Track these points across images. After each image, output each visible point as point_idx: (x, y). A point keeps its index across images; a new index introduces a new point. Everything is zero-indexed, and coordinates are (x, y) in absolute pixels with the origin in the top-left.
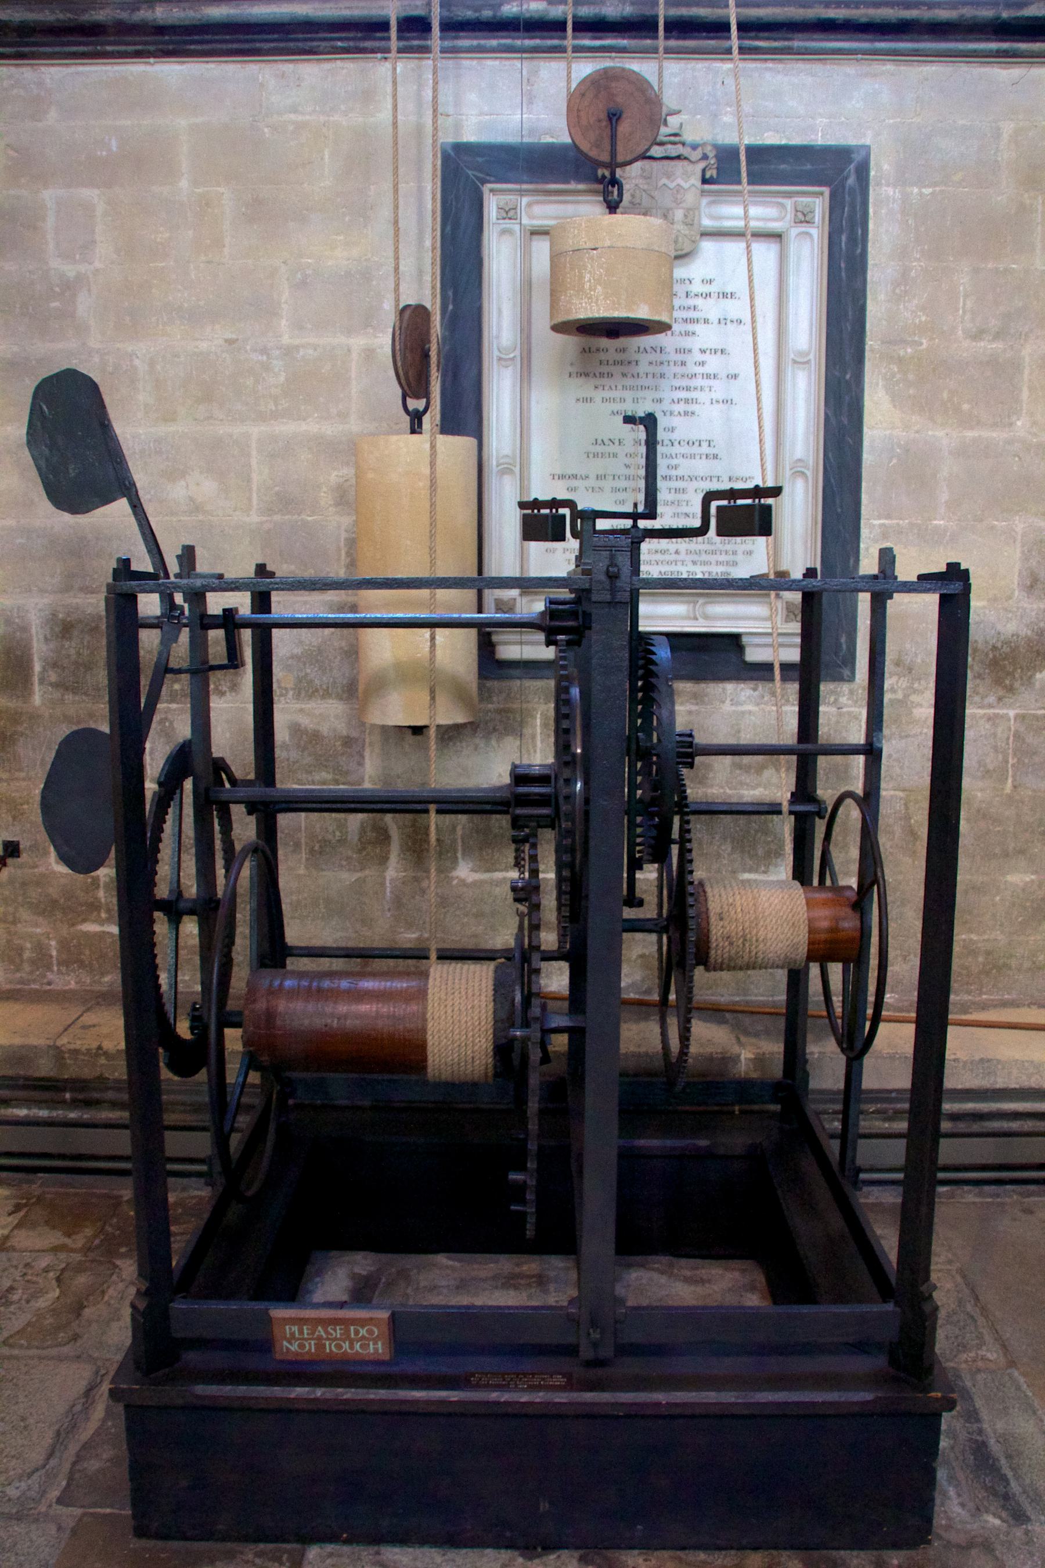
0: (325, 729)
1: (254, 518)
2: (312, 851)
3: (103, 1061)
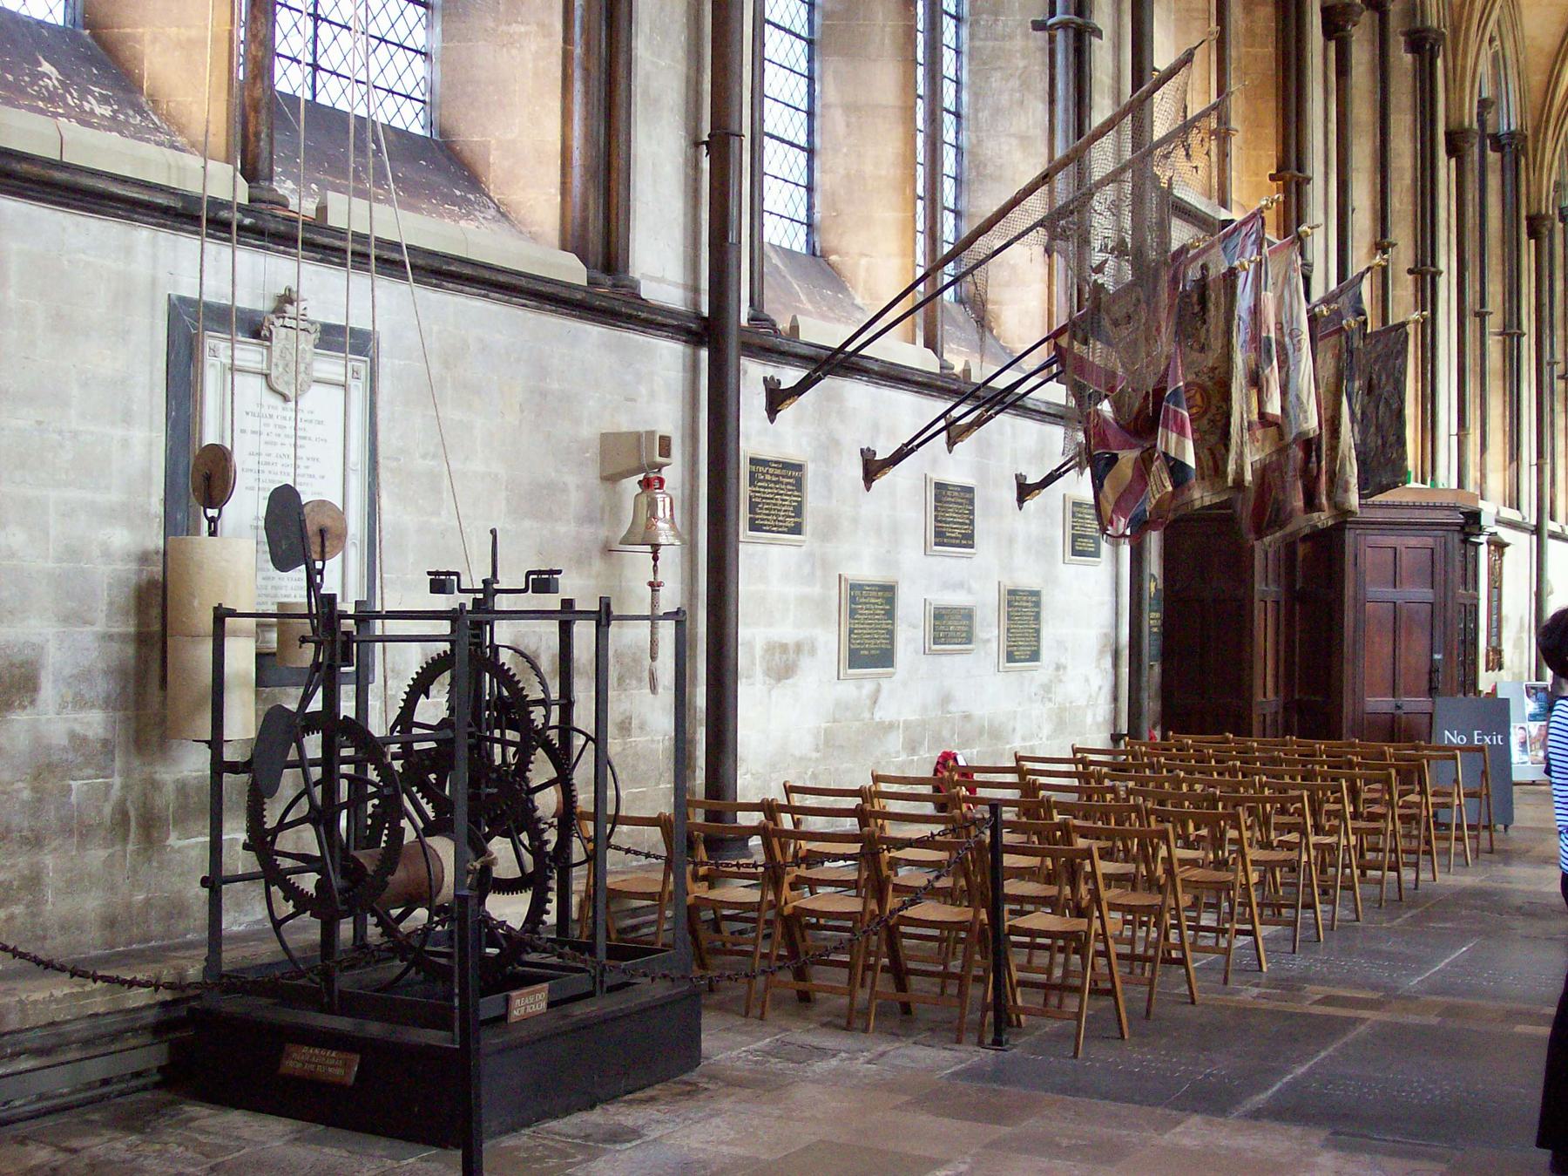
0: (90, 734)
1: (51, 565)
2: (81, 835)
3: (54, 1006)
